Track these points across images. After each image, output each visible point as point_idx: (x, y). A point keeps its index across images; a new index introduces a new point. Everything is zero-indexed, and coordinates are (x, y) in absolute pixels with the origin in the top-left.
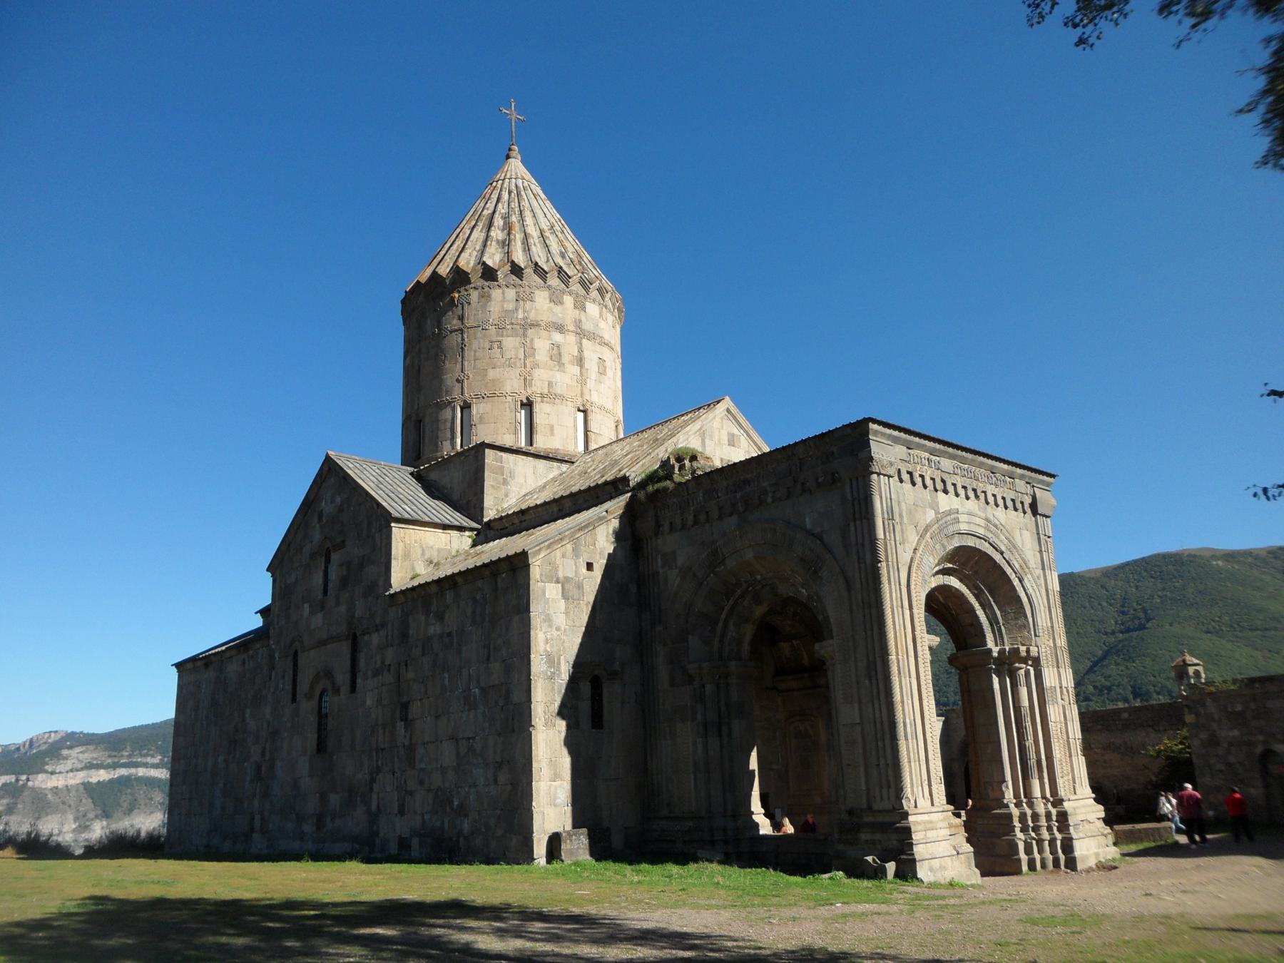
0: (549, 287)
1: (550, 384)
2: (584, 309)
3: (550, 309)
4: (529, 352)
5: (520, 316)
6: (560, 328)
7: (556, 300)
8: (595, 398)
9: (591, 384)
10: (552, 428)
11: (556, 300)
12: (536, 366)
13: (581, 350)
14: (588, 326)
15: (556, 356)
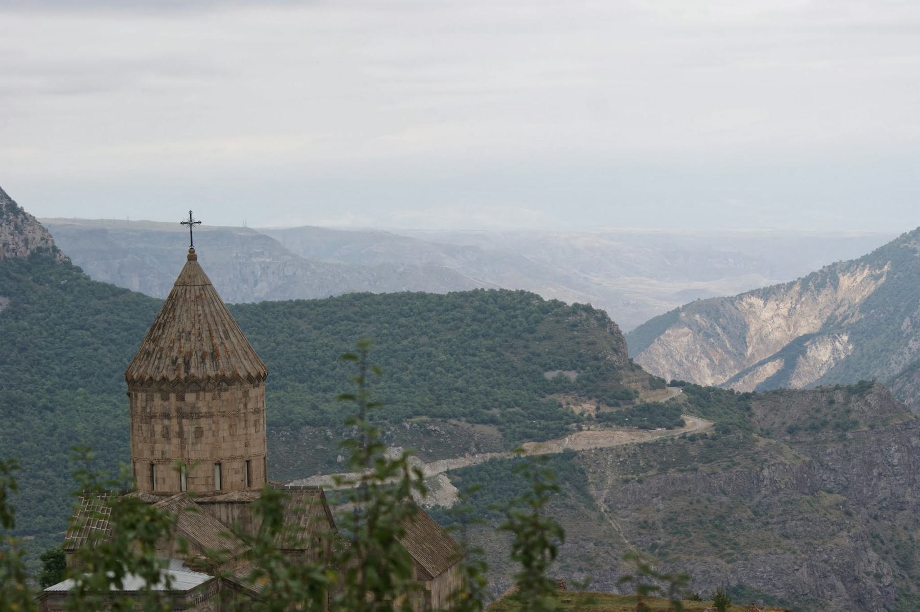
0: (161, 391)
1: (163, 453)
2: (183, 399)
3: (162, 405)
4: (153, 433)
5: (148, 410)
6: (167, 416)
7: (166, 398)
8: (193, 455)
9: (189, 447)
10: (164, 479)
11: (166, 398)
12: (155, 442)
13: (181, 428)
14: (187, 409)
15: (166, 435)
